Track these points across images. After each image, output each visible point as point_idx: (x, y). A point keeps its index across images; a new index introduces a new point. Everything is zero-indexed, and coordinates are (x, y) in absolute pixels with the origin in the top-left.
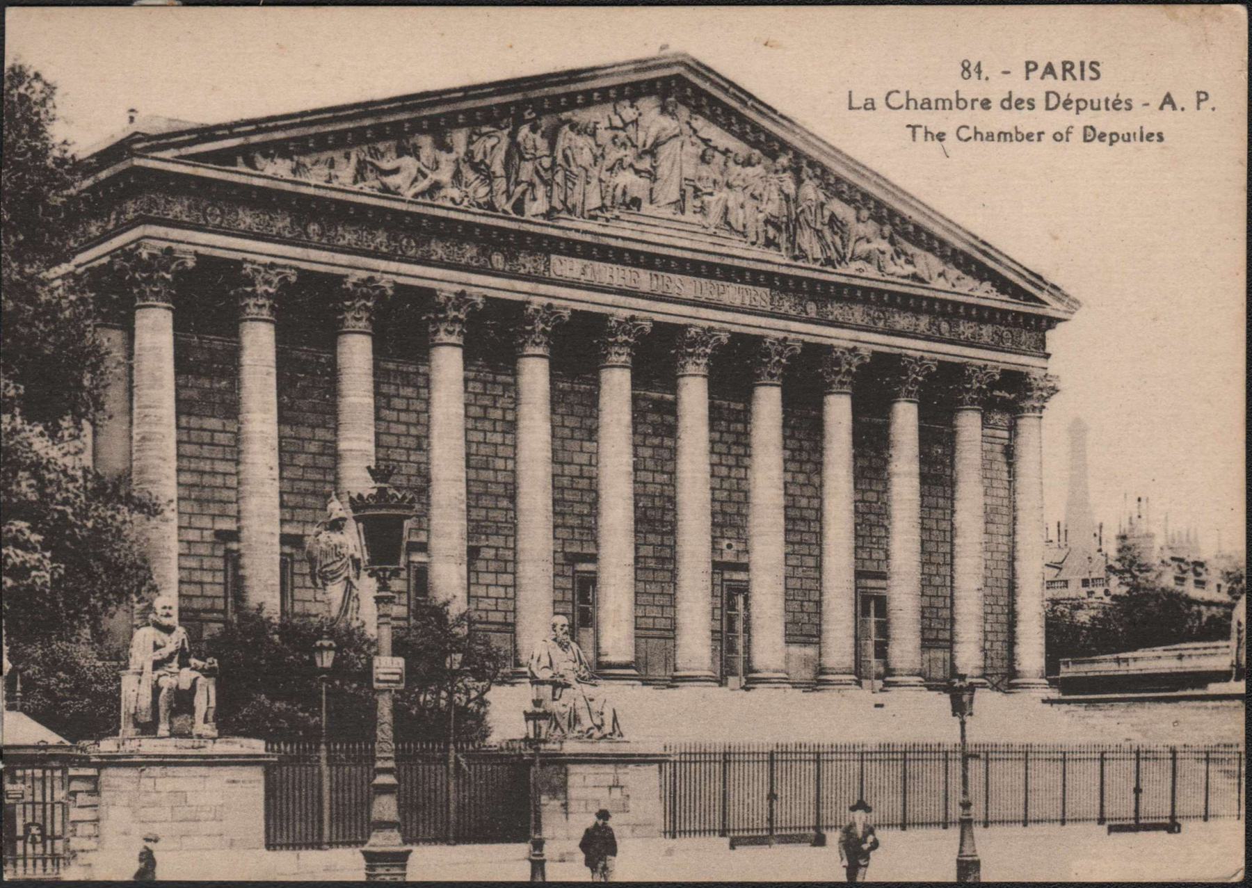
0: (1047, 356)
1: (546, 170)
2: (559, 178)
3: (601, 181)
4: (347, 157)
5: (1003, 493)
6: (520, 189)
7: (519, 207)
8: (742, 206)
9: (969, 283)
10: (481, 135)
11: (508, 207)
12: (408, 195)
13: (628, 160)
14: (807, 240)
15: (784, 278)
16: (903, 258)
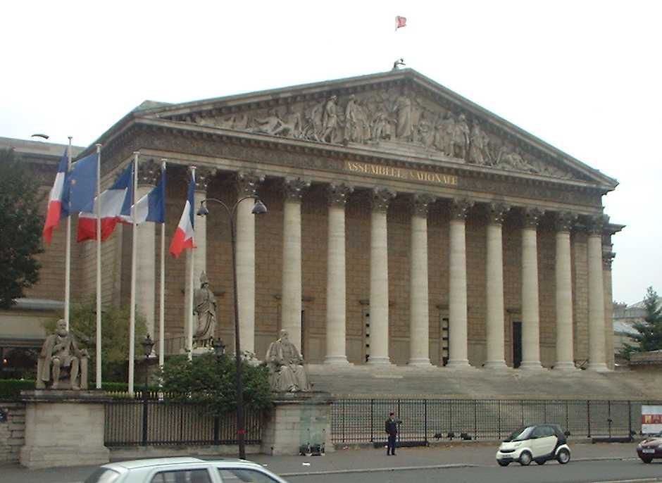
0: (604, 208)
1: (342, 122)
3: (370, 126)
4: (242, 118)
7: (328, 139)
8: (443, 138)
9: (560, 174)
10: (309, 106)
11: (323, 140)
12: (273, 134)
13: (383, 117)
14: (476, 154)
15: (464, 171)
16: (526, 162)
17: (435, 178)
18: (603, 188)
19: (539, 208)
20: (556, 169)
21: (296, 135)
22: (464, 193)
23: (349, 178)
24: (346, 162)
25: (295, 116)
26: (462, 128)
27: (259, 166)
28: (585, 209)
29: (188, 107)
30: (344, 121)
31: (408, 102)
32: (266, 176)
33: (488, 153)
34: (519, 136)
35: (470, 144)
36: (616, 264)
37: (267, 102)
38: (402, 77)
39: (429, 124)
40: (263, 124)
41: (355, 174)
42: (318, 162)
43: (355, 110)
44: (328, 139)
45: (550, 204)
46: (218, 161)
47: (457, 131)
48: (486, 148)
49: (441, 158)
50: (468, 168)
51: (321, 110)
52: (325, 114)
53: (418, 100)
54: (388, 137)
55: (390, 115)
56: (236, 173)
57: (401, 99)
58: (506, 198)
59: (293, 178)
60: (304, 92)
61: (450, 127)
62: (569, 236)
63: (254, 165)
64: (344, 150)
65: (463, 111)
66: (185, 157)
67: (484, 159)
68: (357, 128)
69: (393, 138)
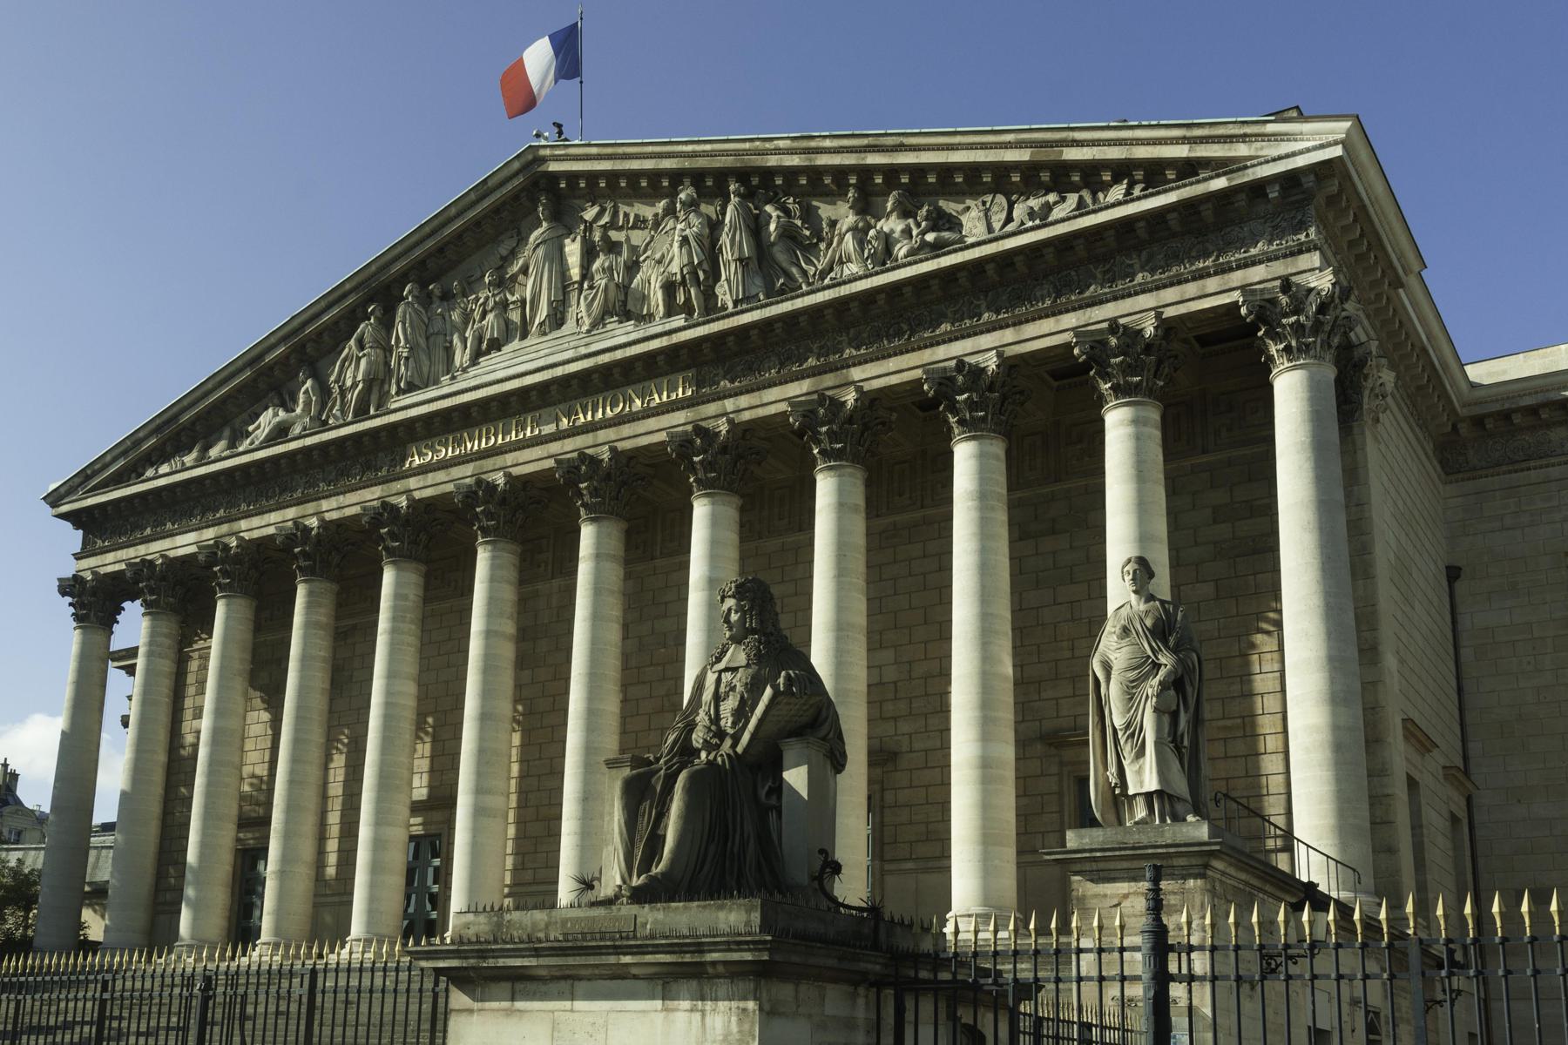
22: (711, 409)
23: (413, 483)
29: (124, 453)
33: (784, 265)
46: (181, 540)
58: (857, 373)
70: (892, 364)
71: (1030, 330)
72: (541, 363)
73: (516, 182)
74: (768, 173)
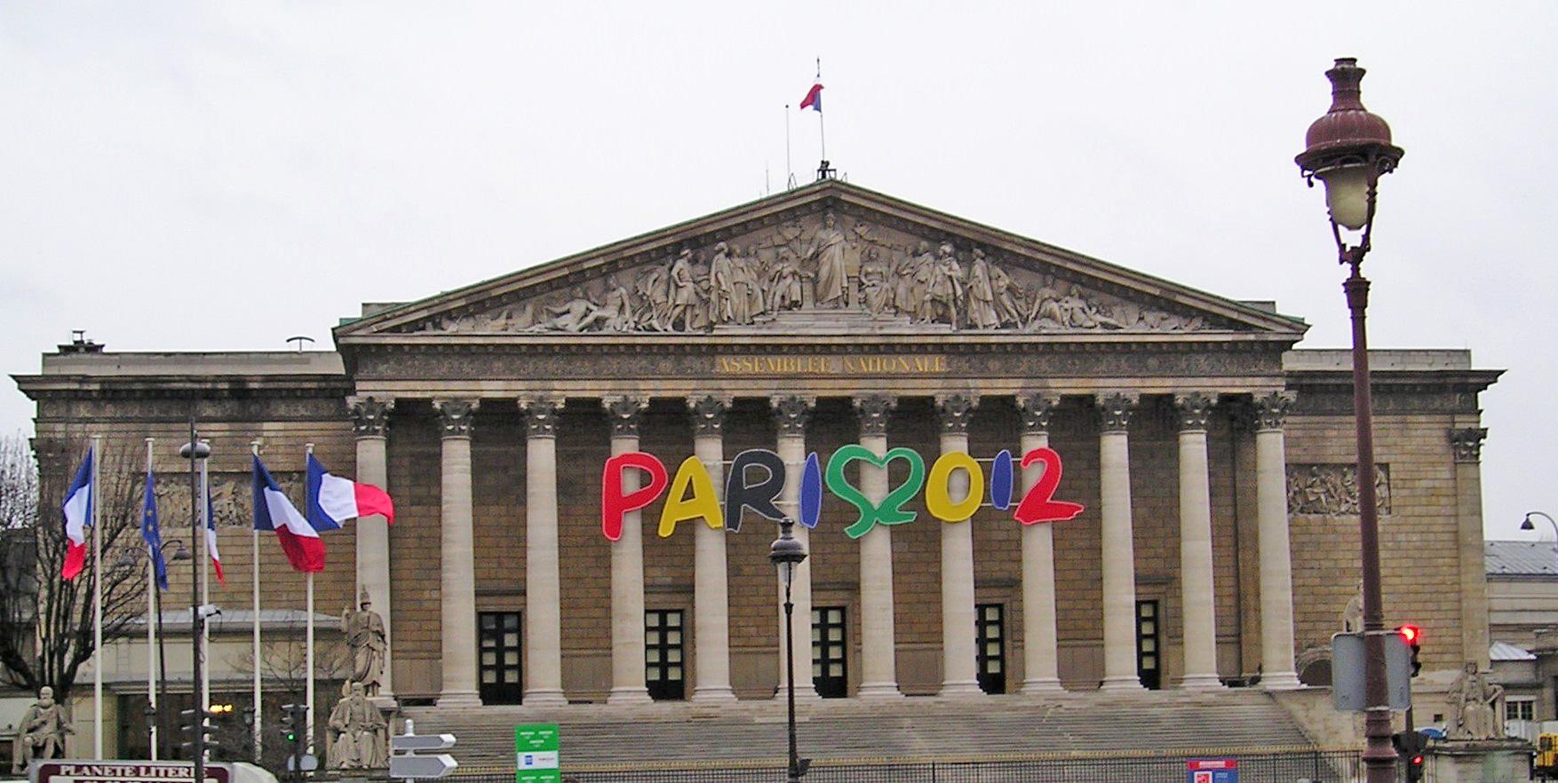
2: (714, 297)
5: (1447, 475)
6: (678, 310)
7: (679, 325)
11: (670, 327)
13: (786, 272)
17: (898, 364)
18: (1272, 338)
19: (1127, 394)
20: (1165, 315)
21: (619, 323)
22: (960, 383)
23: (724, 384)
24: (718, 359)
25: (616, 293)
26: (945, 269)
27: (557, 384)
28: (1238, 381)
30: (707, 291)
31: (834, 237)
32: (567, 400)
34: (1069, 265)
35: (966, 295)
36: (1487, 449)
37: (566, 276)
38: (818, 197)
39: (884, 269)
40: (558, 315)
41: (735, 377)
42: (666, 365)
43: (726, 270)
44: (679, 325)
45: (1158, 382)
46: (484, 385)
47: (939, 273)
48: (1004, 298)
49: (903, 327)
50: (961, 340)
51: (665, 277)
52: (673, 285)
53: (859, 230)
54: (796, 304)
55: (804, 263)
56: (514, 401)
57: (822, 234)
58: (1052, 383)
59: (619, 399)
60: (627, 253)
61: (924, 269)
62: (1204, 438)
63: (548, 385)
64: (706, 341)
65: (950, 237)
66: (428, 385)
67: (999, 317)
68: (736, 300)
69: (808, 305)
70: (1073, 382)
71: (1149, 382)
72: (845, 332)
73: (813, 198)
74: (998, 249)
